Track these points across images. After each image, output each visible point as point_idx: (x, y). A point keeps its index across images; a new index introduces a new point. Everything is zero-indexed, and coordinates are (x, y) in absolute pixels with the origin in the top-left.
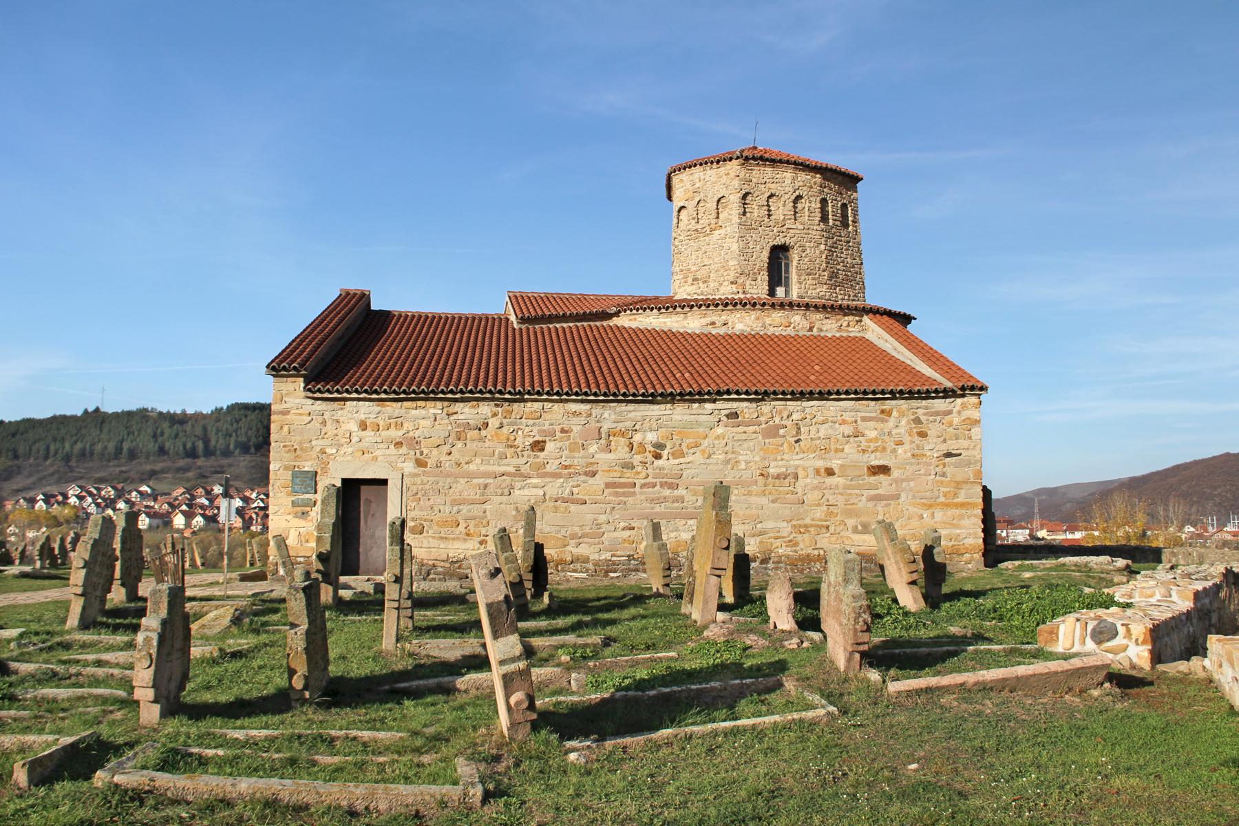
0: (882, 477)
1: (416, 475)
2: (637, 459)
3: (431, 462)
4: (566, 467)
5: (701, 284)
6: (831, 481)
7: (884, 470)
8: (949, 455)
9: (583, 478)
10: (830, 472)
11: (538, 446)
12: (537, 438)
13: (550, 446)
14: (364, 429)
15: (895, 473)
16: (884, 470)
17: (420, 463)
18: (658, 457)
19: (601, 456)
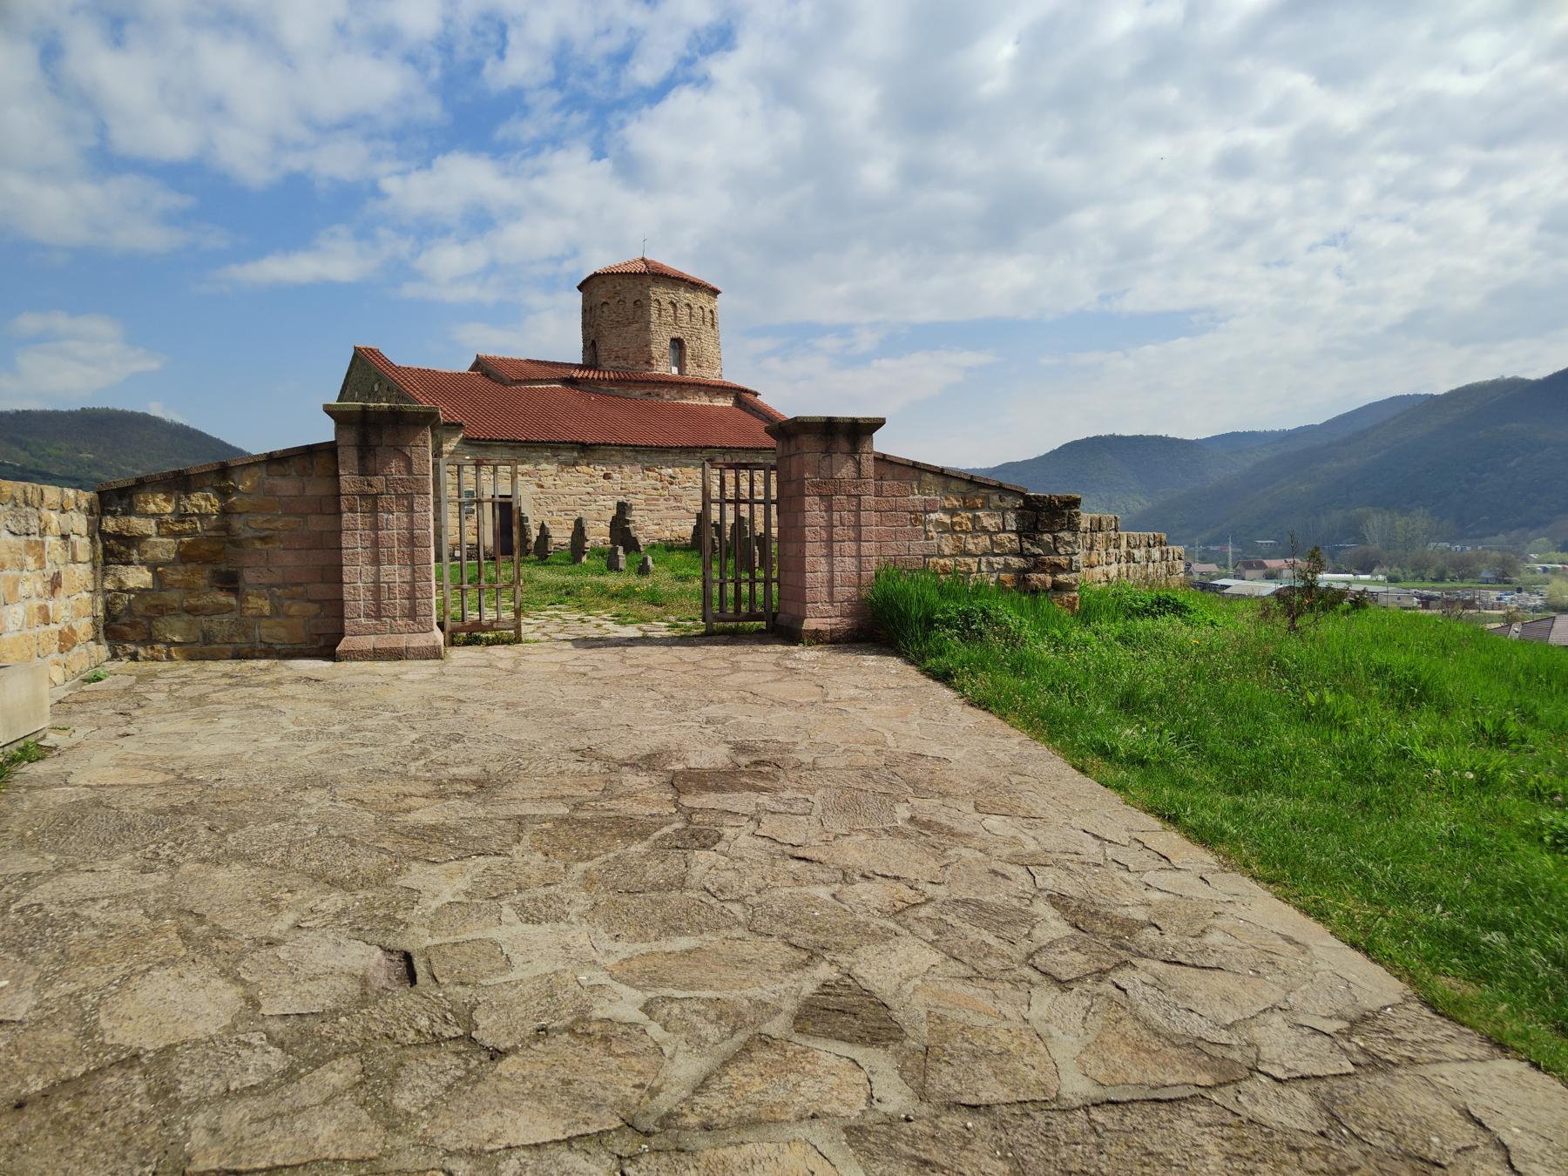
2: (659, 485)
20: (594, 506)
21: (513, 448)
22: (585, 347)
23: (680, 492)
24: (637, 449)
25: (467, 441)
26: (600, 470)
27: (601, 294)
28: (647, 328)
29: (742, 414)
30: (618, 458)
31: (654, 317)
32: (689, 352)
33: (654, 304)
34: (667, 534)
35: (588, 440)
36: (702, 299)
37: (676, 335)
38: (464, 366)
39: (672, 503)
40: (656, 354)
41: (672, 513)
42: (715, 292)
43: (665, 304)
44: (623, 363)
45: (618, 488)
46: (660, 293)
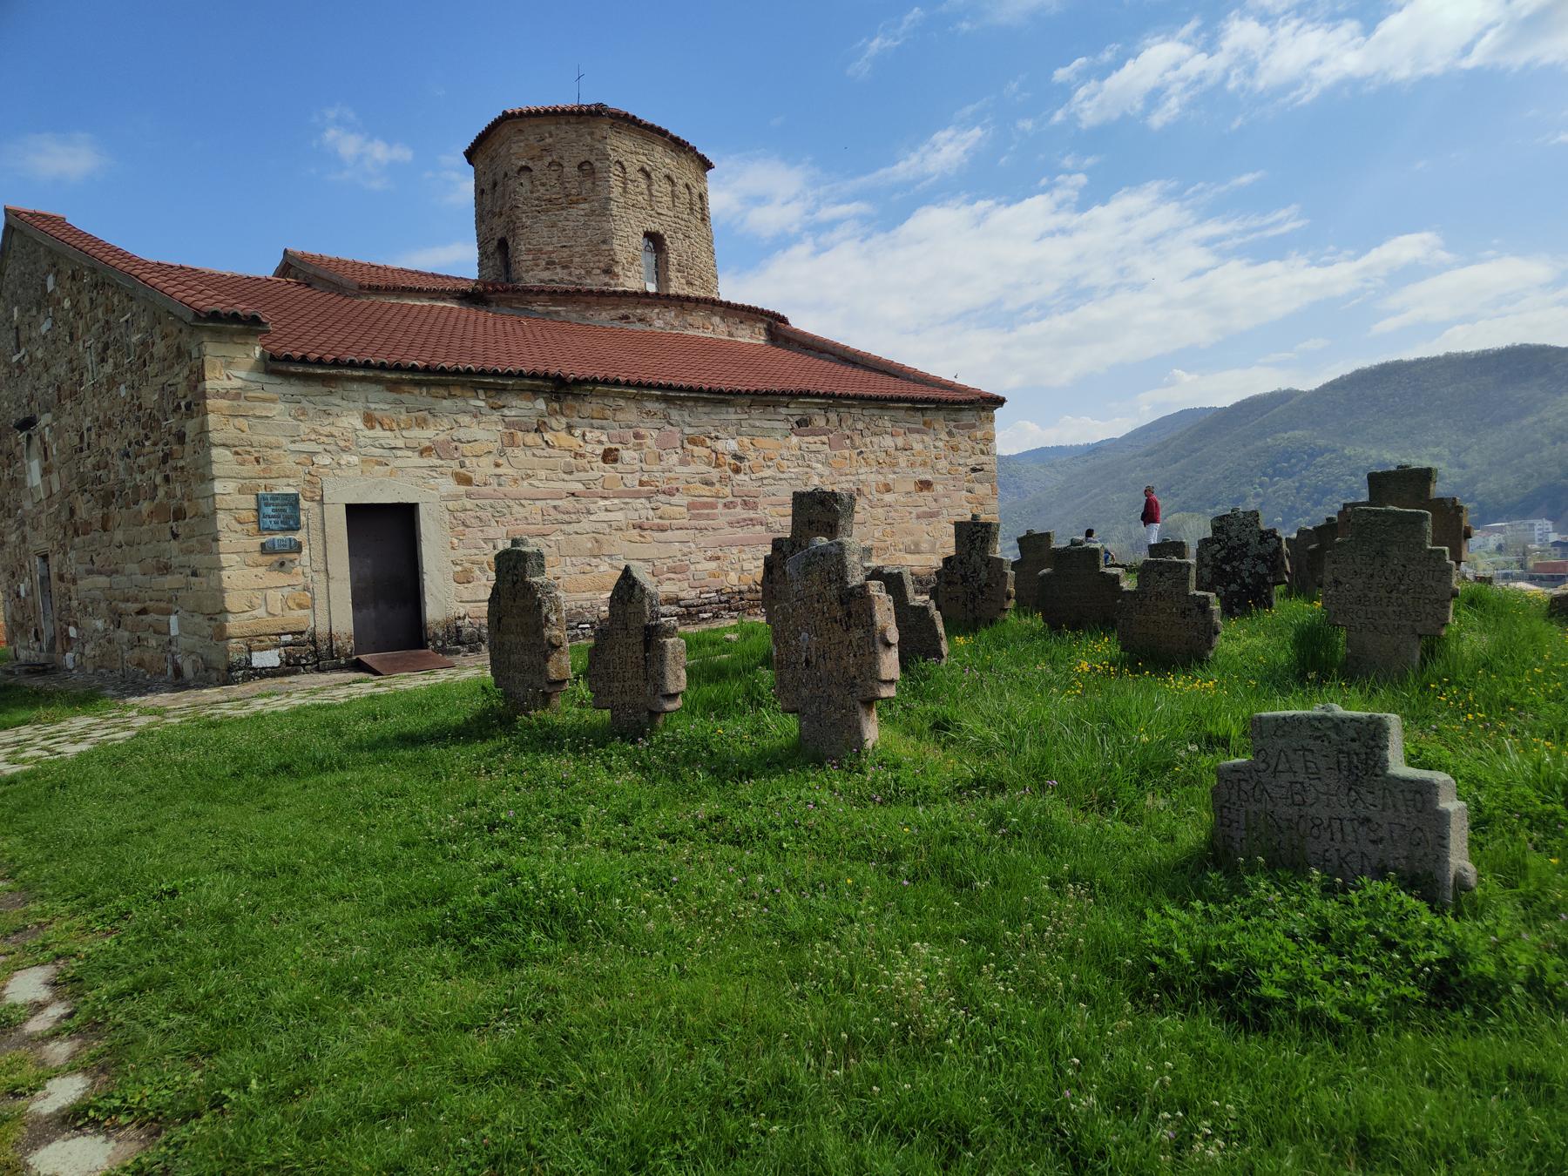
0: (925, 493)
1: (457, 497)
2: (714, 474)
3: (477, 478)
4: (641, 484)
5: (559, 270)
6: (888, 498)
7: (925, 485)
8: (974, 470)
9: (661, 497)
10: (888, 489)
11: (609, 456)
12: (608, 445)
13: (626, 455)
14: (373, 428)
15: (939, 488)
16: (925, 485)
17: (465, 480)
18: (737, 471)
19: (679, 469)
20: (585, 525)
21: (393, 386)
22: (483, 255)
23: (752, 487)
24: (673, 395)
25: (276, 366)
26: (596, 440)
27: (517, 150)
28: (603, 211)
29: (781, 353)
30: (630, 414)
31: (616, 192)
32: (673, 258)
33: (616, 169)
34: (733, 578)
35: (572, 370)
36: (685, 173)
37: (653, 227)
38: (265, 266)
39: (740, 512)
40: (621, 257)
41: (741, 533)
42: (707, 165)
43: (632, 171)
44: (560, 273)
45: (632, 481)
46: (622, 147)
